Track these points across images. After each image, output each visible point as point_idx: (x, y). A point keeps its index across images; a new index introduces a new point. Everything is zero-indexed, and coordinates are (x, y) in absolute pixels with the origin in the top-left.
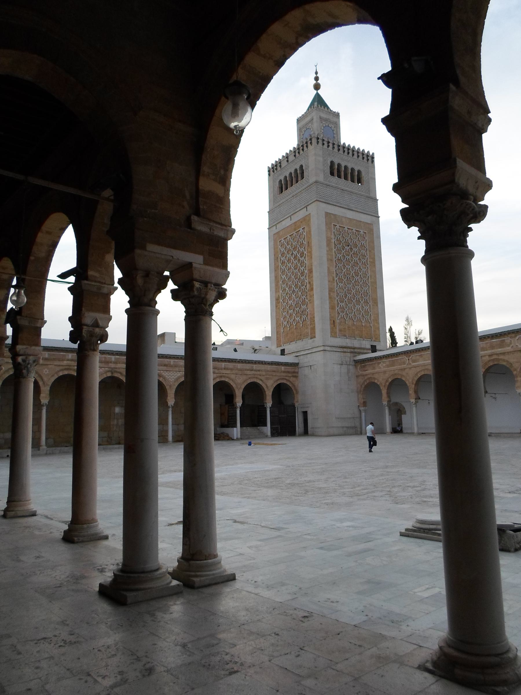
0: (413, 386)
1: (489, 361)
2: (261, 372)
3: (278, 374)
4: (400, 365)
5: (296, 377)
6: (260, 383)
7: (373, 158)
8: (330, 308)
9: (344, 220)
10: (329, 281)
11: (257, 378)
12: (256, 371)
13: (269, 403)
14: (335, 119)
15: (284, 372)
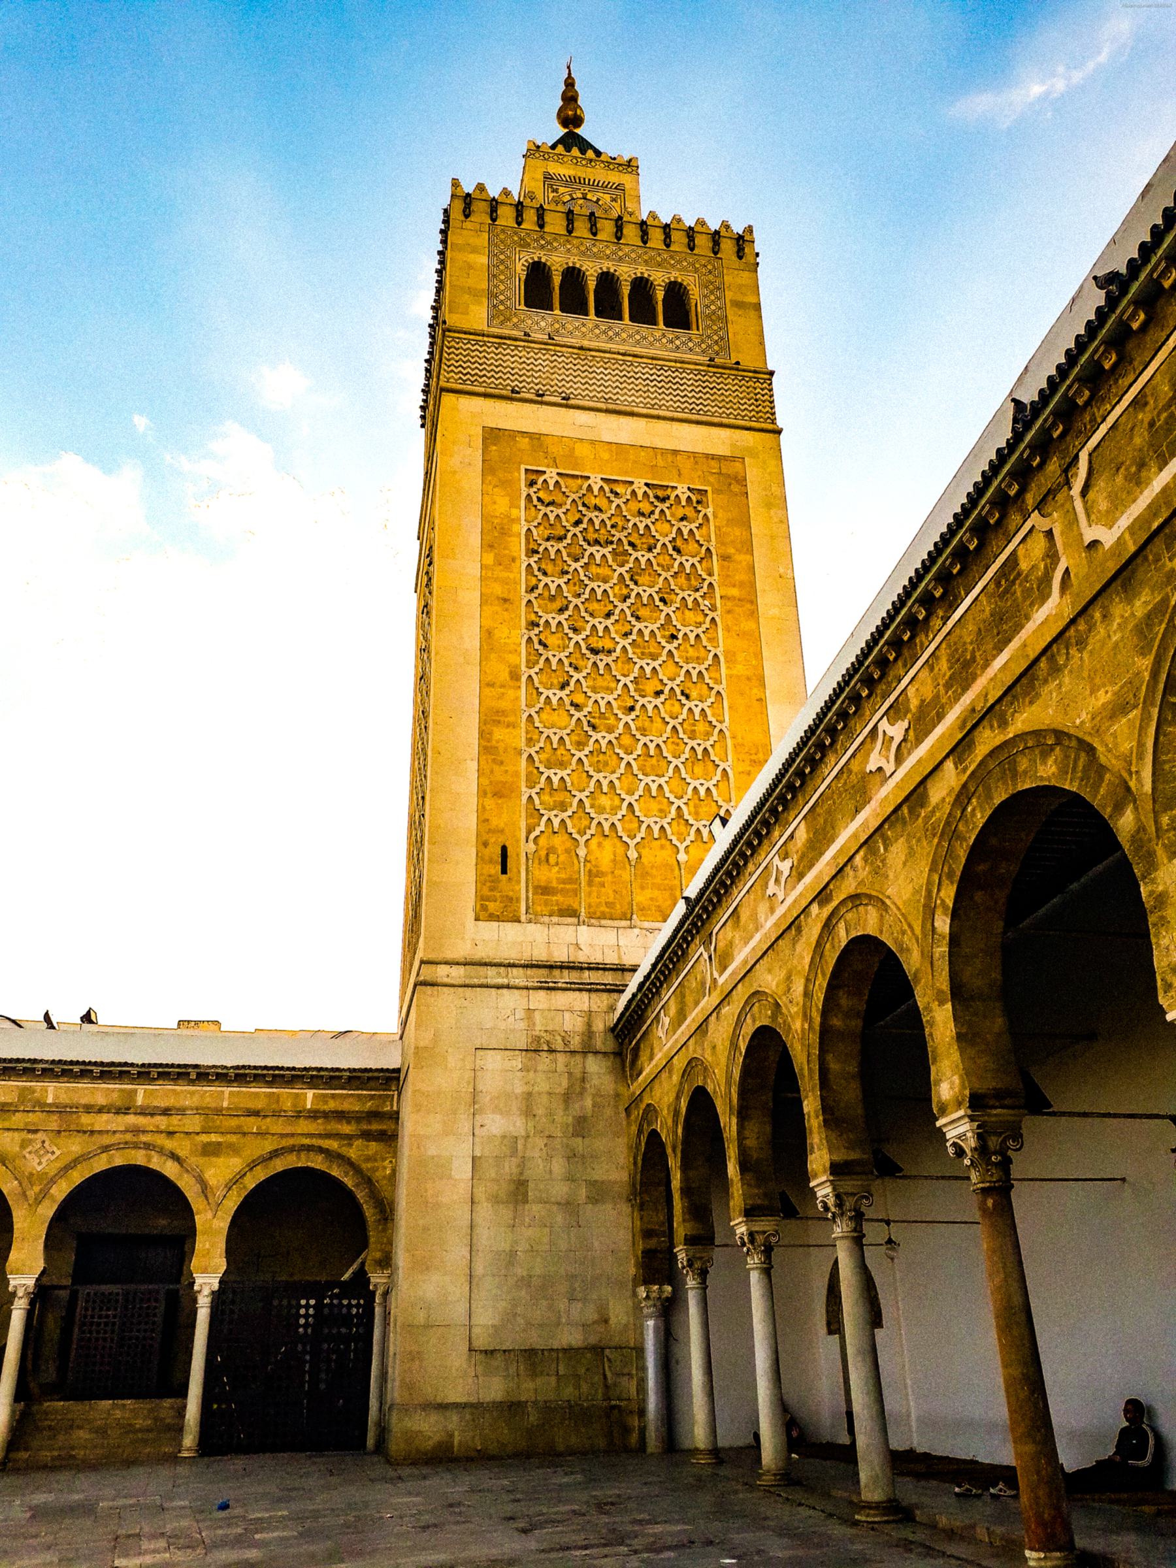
0: (734, 1120)
1: (963, 797)
2: (175, 1120)
3: (278, 1127)
4: (697, 1003)
5: (389, 1138)
6: (170, 1169)
7: (742, 242)
8: (482, 793)
9: (582, 451)
10: (487, 684)
11: (148, 1146)
12: (143, 1112)
13: (207, 1274)
14: (614, 177)
15: (314, 1115)
